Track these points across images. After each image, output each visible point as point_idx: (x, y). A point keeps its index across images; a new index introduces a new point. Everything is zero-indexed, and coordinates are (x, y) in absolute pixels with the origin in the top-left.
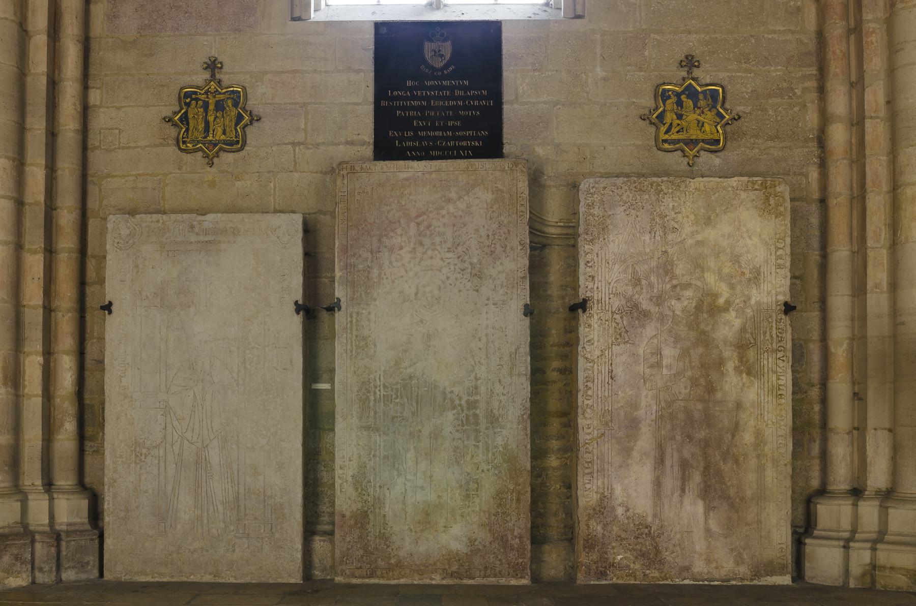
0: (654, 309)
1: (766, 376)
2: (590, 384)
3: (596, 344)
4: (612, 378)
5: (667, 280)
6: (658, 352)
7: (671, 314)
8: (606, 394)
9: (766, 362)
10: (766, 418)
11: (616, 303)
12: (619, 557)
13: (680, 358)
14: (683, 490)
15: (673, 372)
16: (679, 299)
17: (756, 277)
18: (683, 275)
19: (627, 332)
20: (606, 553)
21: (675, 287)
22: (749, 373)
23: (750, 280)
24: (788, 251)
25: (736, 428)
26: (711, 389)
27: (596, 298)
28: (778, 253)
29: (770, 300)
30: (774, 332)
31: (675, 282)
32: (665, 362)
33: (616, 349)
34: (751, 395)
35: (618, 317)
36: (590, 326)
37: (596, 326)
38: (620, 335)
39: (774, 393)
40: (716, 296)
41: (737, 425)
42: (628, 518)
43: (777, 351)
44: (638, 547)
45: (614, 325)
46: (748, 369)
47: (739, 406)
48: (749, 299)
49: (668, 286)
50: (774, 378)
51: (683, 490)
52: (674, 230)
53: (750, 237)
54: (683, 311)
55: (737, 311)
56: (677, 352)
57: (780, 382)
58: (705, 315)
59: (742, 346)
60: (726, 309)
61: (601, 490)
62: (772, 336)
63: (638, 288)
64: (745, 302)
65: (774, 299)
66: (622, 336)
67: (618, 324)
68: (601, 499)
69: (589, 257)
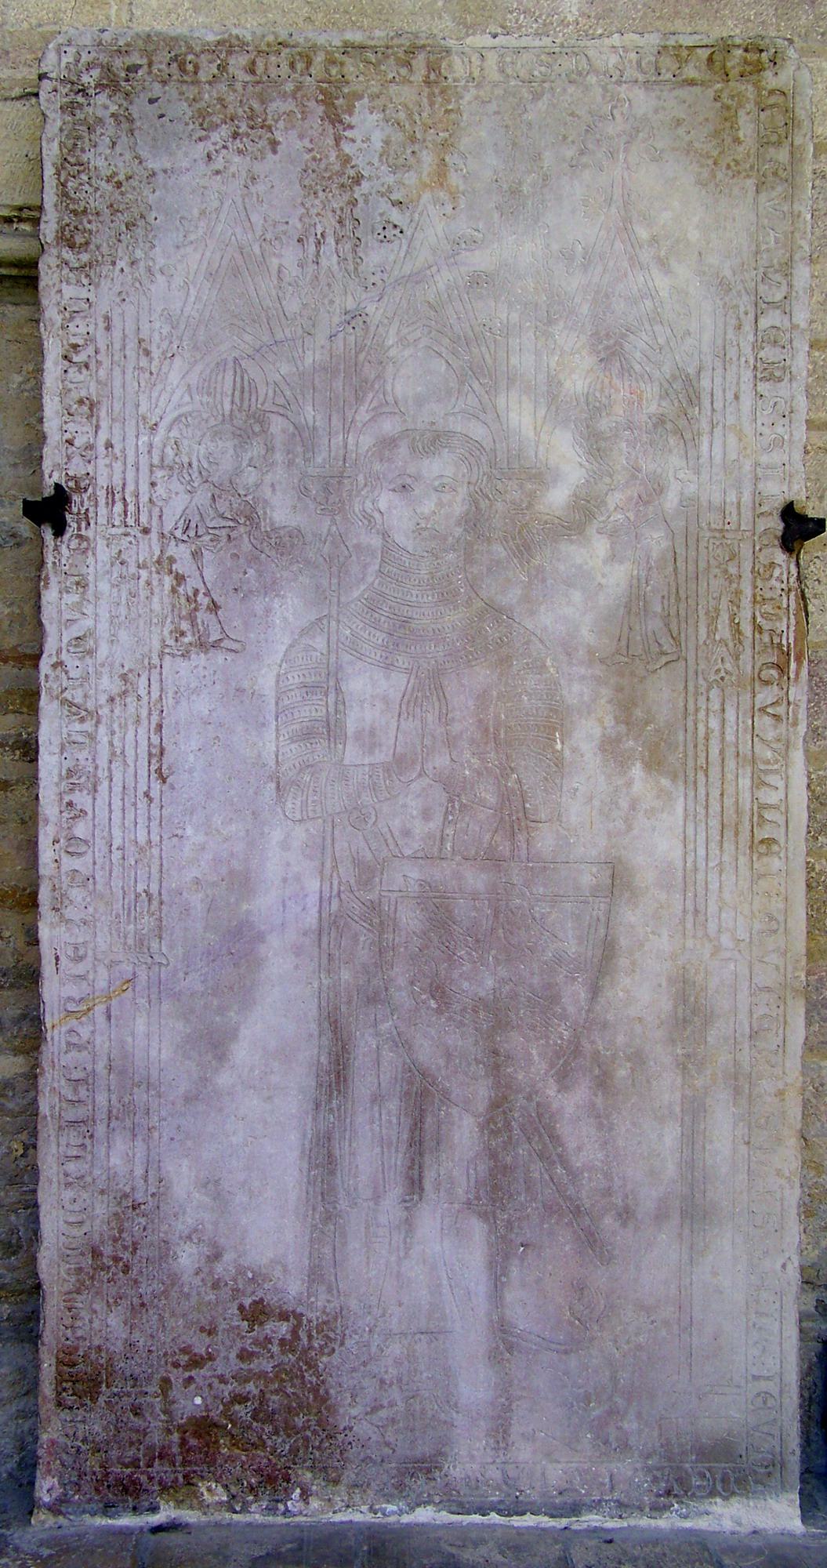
1: (715, 772)
2: (81, 799)
3: (103, 651)
6: (327, 683)
7: (376, 542)
8: (142, 837)
9: (714, 724)
10: (712, 926)
11: (177, 502)
13: (410, 703)
14: (415, 1184)
15: (381, 756)
17: (684, 409)
19: (214, 607)
21: (388, 444)
22: (654, 763)
23: (661, 421)
25: (604, 961)
26: (515, 817)
27: (102, 481)
28: (764, 323)
30: (745, 615)
31: (389, 426)
35: (181, 553)
36: (82, 585)
37: (104, 586)
38: (192, 618)
39: (745, 835)
40: (540, 477)
41: (608, 950)
47: (617, 880)
48: (660, 490)
49: (367, 441)
50: (745, 782)
51: (415, 1184)
52: (389, 231)
53: (663, 264)
54: (419, 530)
56: (395, 684)
58: (499, 551)
62: (737, 630)
63: (256, 449)
65: (746, 498)
66: (200, 624)
69: (79, 329)
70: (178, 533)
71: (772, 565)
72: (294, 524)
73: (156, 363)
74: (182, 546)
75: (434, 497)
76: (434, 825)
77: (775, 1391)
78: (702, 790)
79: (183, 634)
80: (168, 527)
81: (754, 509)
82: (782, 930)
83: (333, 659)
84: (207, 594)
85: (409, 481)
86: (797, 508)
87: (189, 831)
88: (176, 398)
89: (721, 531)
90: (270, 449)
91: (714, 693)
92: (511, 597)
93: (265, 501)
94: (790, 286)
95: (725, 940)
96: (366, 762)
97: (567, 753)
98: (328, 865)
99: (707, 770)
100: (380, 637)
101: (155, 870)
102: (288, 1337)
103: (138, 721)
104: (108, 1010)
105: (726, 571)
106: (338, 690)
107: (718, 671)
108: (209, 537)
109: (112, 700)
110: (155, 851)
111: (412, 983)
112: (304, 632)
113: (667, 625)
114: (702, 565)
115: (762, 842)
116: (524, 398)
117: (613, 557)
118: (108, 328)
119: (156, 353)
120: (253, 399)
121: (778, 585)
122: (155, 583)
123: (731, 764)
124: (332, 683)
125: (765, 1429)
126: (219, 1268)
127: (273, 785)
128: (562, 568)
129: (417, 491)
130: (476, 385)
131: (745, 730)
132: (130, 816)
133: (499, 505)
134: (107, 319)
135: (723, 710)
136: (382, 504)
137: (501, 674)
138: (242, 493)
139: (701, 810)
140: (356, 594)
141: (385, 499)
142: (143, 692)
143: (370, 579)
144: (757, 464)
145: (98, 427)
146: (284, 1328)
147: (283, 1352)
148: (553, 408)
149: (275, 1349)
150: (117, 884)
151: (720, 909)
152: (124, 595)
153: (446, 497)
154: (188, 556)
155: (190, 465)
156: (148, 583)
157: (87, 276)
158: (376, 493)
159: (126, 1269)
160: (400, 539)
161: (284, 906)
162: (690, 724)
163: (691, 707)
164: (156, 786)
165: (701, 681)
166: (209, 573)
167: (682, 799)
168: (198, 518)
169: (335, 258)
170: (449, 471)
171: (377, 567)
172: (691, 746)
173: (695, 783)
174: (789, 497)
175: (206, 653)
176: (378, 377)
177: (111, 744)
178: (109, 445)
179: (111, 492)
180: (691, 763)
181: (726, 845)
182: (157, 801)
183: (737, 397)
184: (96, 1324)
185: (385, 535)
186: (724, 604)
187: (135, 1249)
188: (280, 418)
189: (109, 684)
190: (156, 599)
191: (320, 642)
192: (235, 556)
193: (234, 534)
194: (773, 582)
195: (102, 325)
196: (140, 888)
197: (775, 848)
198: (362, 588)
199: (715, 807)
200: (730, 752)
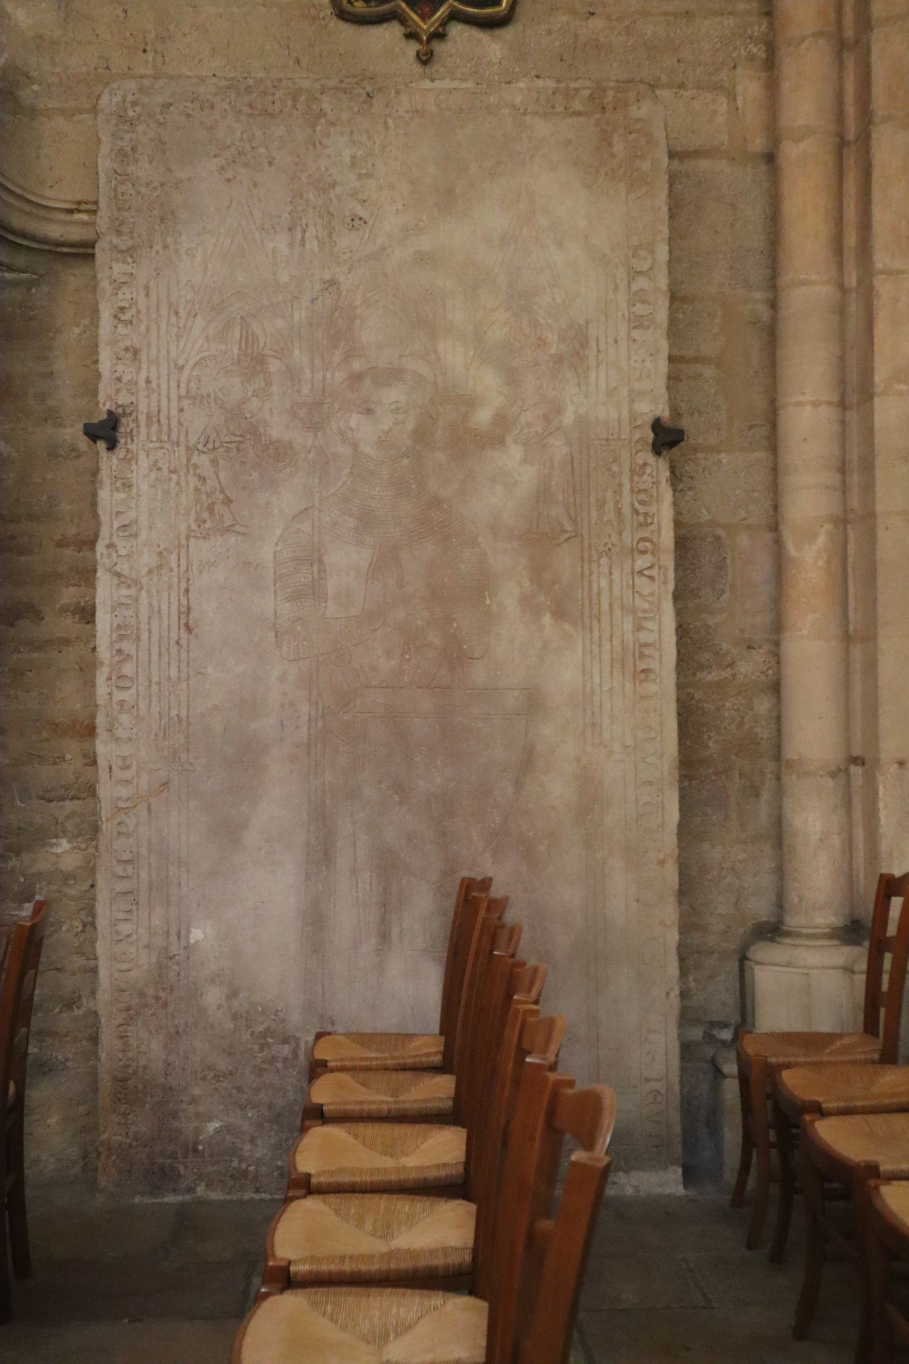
0: (301, 438)
1: (605, 620)
2: (128, 647)
3: (143, 535)
4: (189, 629)
5: (336, 359)
6: (314, 557)
8: (174, 673)
9: (604, 583)
10: (606, 735)
11: (199, 422)
12: (213, 1126)
14: (384, 937)
16: (369, 412)
17: (577, 351)
19: (228, 501)
20: (175, 1115)
21: (356, 378)
22: (559, 614)
23: (559, 359)
24: (663, 282)
25: (528, 761)
26: (456, 656)
27: (143, 408)
28: (635, 288)
29: (614, 414)
30: (627, 499)
31: (357, 365)
32: (331, 585)
33: (201, 550)
34: (565, 674)
35: (203, 460)
36: (127, 486)
37: (144, 487)
38: (211, 509)
40: (470, 402)
42: (235, 1017)
43: (636, 551)
44: (264, 1097)
45: (193, 481)
46: (562, 604)
47: (534, 703)
49: (340, 376)
50: (628, 626)
51: (384, 937)
52: (356, 222)
53: (560, 245)
54: (380, 443)
55: (525, 444)
56: (363, 557)
57: (644, 637)
58: (440, 456)
59: (538, 539)
60: (496, 436)
61: (160, 942)
62: (619, 513)
63: (258, 383)
64: (546, 418)
65: (625, 413)
66: (217, 513)
67: (203, 479)
68: (160, 965)
69: (124, 297)
70: (200, 446)
71: (645, 464)
73: (182, 321)
74: (203, 456)
77: (663, 1091)
78: (596, 634)
79: (204, 521)
80: (192, 442)
81: (630, 423)
82: (658, 738)
84: (222, 491)
85: (373, 406)
86: (663, 421)
87: (210, 670)
88: (197, 346)
89: (607, 439)
90: (269, 384)
91: (604, 561)
93: (265, 421)
94: (654, 260)
95: (617, 747)
97: (494, 607)
98: (314, 694)
99: (599, 619)
100: (352, 522)
101: (183, 699)
102: (290, 1056)
103: (170, 587)
104: (149, 805)
105: (609, 470)
106: (321, 562)
107: (606, 544)
108: (222, 450)
109: (150, 572)
110: (184, 685)
111: (380, 782)
113: (567, 511)
114: (592, 465)
115: (643, 671)
117: (525, 461)
118: (147, 295)
119: (183, 313)
120: (255, 348)
121: (649, 479)
122: (183, 483)
123: (618, 613)
125: (656, 1118)
126: (236, 1004)
127: (274, 634)
129: (379, 413)
131: (628, 587)
132: (165, 659)
134: (147, 288)
135: (611, 574)
136: (353, 423)
138: (248, 416)
139: (595, 648)
141: (355, 420)
142: (174, 565)
143: (344, 479)
144: (631, 391)
145: (140, 368)
146: (286, 1050)
147: (286, 1068)
149: (280, 1065)
150: (155, 709)
151: (612, 722)
152: (160, 492)
153: (401, 417)
154: (208, 463)
155: (209, 395)
156: (178, 484)
157: (131, 256)
158: (348, 415)
159: (166, 1005)
161: (282, 725)
162: (586, 584)
163: (587, 572)
164: (184, 635)
165: (594, 552)
166: (222, 475)
167: (581, 641)
168: (214, 435)
169: (315, 243)
170: (403, 398)
171: (349, 470)
172: (587, 601)
173: (591, 628)
174: (658, 413)
175: (222, 535)
177: (150, 604)
178: (148, 381)
179: (149, 417)
180: (587, 611)
181: (615, 674)
182: (185, 646)
183: (616, 341)
184: (143, 1048)
185: (355, 446)
186: (609, 495)
187: (172, 990)
188: (276, 360)
189: (147, 559)
190: (183, 496)
191: (306, 527)
192: (243, 463)
193: (241, 447)
194: (645, 477)
195: (142, 293)
196: (174, 713)
197: (652, 676)
198: (339, 484)
199: (607, 647)
200: (616, 606)
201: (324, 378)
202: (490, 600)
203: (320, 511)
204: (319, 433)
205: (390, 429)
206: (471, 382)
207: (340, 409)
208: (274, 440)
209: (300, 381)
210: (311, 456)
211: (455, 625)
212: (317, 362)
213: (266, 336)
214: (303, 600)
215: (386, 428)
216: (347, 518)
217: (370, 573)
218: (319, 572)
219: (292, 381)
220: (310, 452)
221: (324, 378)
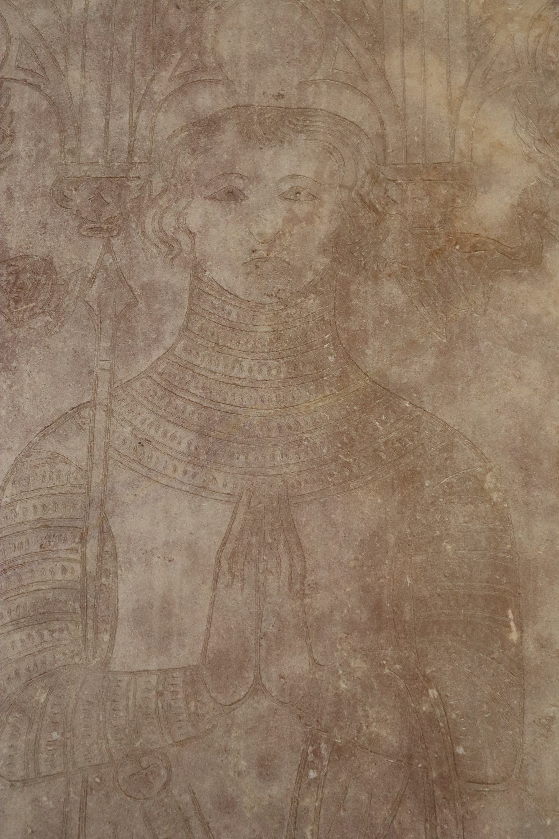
0: (77, 254)
6: (86, 521)
7: (180, 280)
13: (236, 556)
16: (233, 195)
18: (258, 64)
31: (206, 101)
40: (462, 178)
49: (169, 122)
54: (254, 264)
56: (207, 521)
58: (393, 292)
72: (39, 251)
75: (281, 205)
76: (278, 790)
83: (97, 475)
85: (239, 183)
92: (416, 370)
96: (153, 665)
97: (530, 648)
100: (185, 439)
106: (105, 533)
112: (48, 429)
116: (430, 57)
124: (94, 521)
128: (505, 320)
129: (253, 199)
130: (351, 41)
133: (394, 223)
136: (194, 220)
137: (403, 503)
140: (142, 365)
141: (198, 212)
143: (168, 341)
148: (479, 72)
153: (302, 209)
158: (183, 203)
160: (222, 275)
170: (308, 170)
171: (180, 322)
176: (192, 29)
185: (196, 269)
188: (27, 89)
198: (156, 354)
201: (133, 128)
202: (521, 628)
203: (110, 412)
204: (113, 241)
205: (279, 234)
206: (462, 137)
207: (165, 191)
208: (12, 254)
209: (78, 130)
210: (93, 292)
211: (433, 693)
212: (119, 93)
213: (9, 40)
214: (56, 625)
215: (269, 230)
216: (172, 429)
217: (225, 566)
218: (100, 557)
219: (62, 131)
220: (92, 281)
221: (133, 128)
